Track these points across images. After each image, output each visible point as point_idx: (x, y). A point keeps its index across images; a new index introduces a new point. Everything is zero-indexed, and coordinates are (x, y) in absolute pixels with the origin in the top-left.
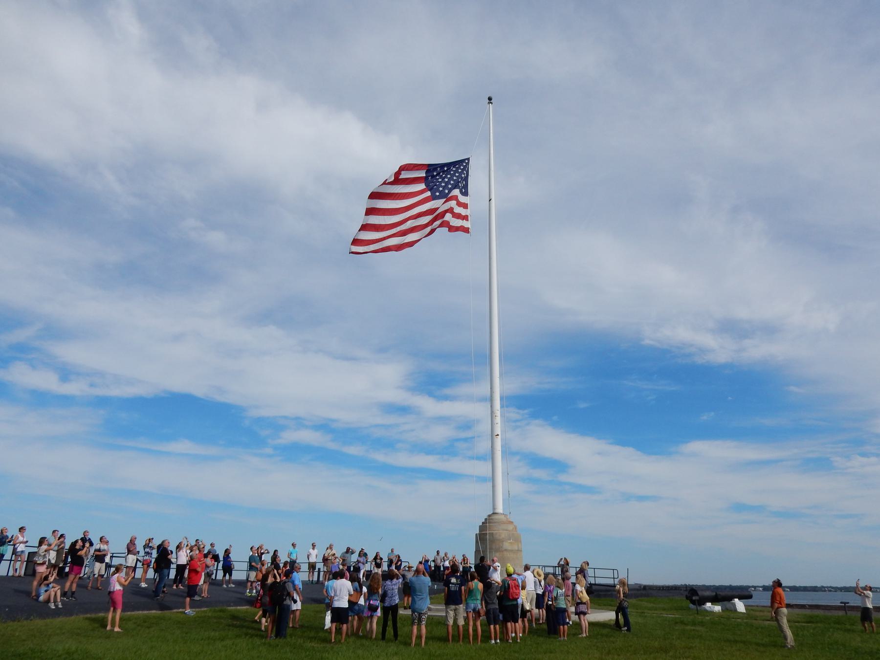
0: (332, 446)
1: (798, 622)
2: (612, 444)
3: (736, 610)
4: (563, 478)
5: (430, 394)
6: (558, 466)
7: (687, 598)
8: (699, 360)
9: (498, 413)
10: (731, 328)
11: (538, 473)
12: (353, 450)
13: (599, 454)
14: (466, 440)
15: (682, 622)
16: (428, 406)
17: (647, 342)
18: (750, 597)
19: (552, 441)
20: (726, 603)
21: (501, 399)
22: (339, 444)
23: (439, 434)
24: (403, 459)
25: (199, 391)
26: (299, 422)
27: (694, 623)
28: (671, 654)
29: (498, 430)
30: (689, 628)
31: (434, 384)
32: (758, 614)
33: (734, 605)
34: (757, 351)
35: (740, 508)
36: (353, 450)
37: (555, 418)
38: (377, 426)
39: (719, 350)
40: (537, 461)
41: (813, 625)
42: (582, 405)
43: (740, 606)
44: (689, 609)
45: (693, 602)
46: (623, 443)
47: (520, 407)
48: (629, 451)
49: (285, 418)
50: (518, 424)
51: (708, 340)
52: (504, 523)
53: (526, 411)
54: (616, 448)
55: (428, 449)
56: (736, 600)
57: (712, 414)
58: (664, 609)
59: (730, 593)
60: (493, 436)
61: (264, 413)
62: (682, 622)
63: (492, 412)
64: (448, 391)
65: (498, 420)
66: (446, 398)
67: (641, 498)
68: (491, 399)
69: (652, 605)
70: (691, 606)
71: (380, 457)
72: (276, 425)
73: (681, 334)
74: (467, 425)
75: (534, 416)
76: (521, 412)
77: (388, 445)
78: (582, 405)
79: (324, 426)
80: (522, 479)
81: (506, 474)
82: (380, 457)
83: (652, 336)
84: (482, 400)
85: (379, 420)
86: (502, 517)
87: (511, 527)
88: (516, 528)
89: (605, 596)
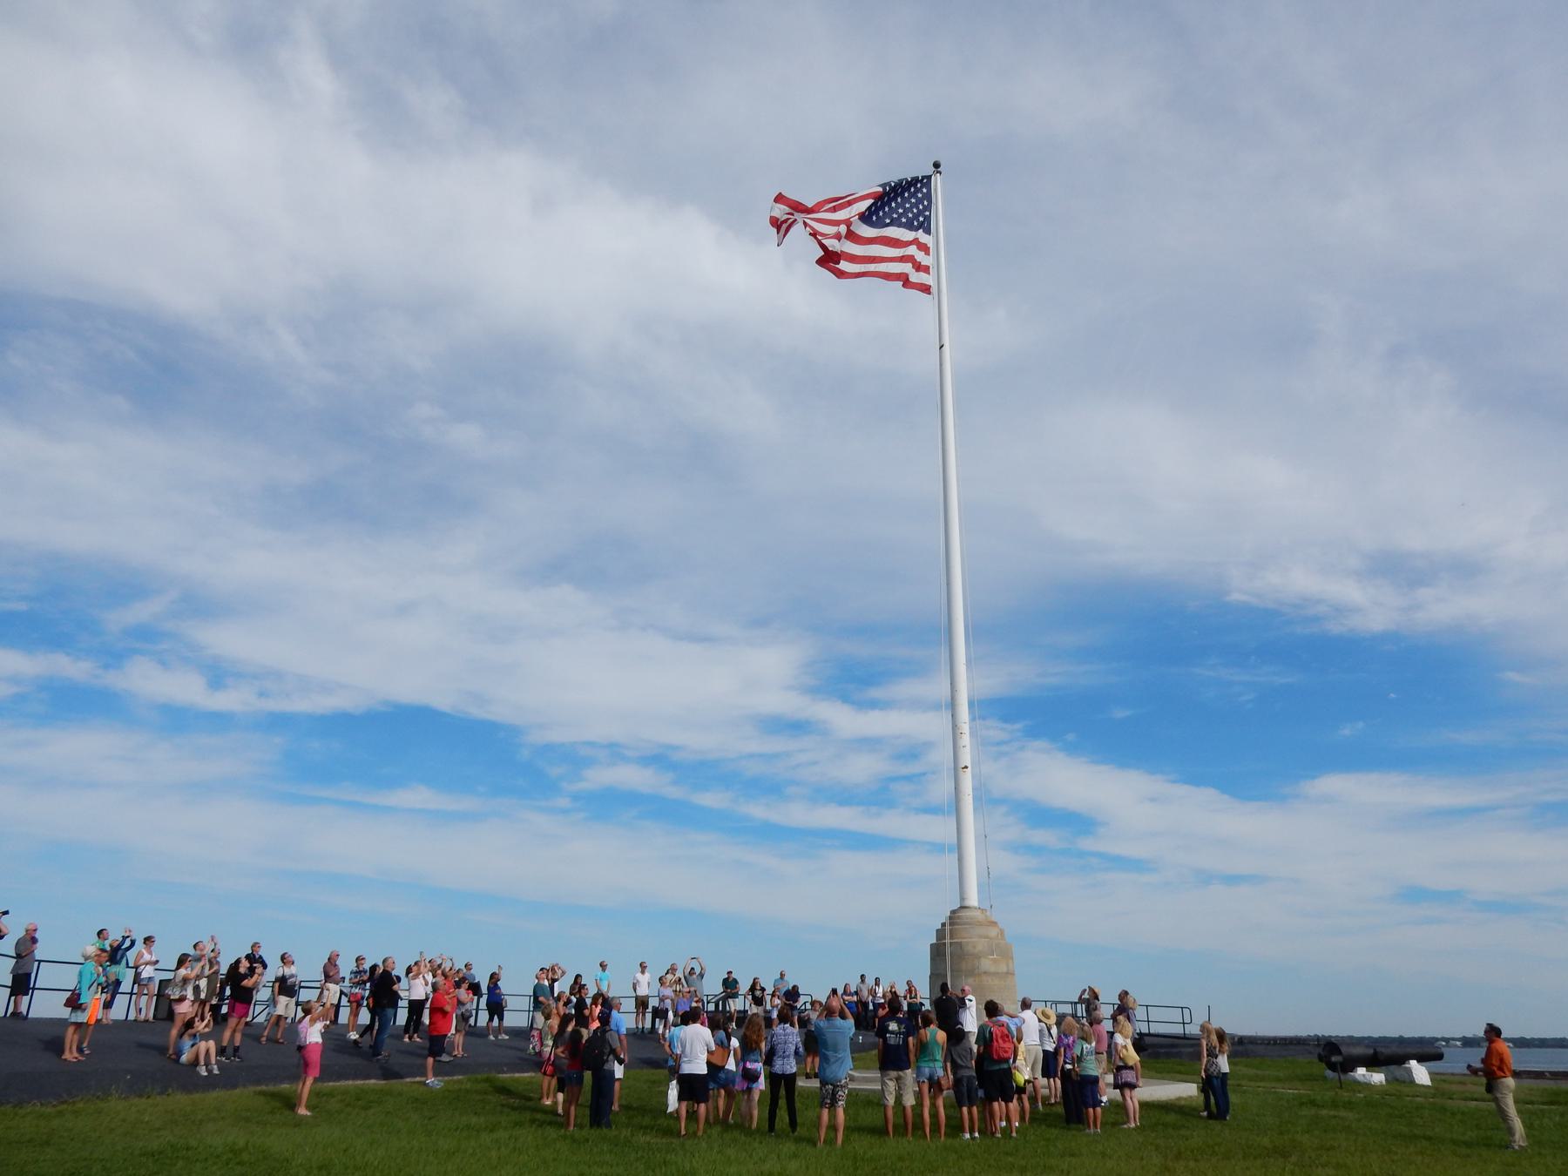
0: (674, 792)
1: (1532, 1103)
2: (1174, 782)
3: (1412, 1081)
4: (1087, 844)
5: (845, 699)
6: (1077, 822)
7: (1321, 1058)
8: (1335, 628)
9: (965, 728)
10: (1390, 567)
11: (1040, 836)
12: (710, 799)
13: (1153, 800)
14: (908, 778)
15: (1313, 1103)
16: (843, 719)
17: (1236, 597)
18: (1439, 1057)
19: (1064, 778)
20: (1392, 1068)
21: (971, 704)
22: (685, 790)
23: (861, 769)
24: (798, 814)
25: (442, 700)
26: (615, 752)
27: (1334, 1105)
28: (1293, 1159)
29: (966, 758)
30: (1324, 1112)
31: (852, 680)
32: (1454, 1088)
33: (1409, 1071)
34: (1442, 608)
35: (1414, 895)
36: (710, 799)
37: (1071, 737)
38: (751, 756)
39: (1372, 608)
40: (1039, 815)
41: (1561, 1108)
42: (1120, 713)
43: (1420, 1073)
44: (1325, 1078)
45: (1332, 1067)
46: (1196, 780)
47: (1006, 719)
48: (1207, 794)
49: (591, 744)
50: (1004, 748)
51: (1351, 592)
52: (980, 924)
53: (1018, 726)
54: (1182, 790)
55: (843, 796)
56: (1413, 1063)
57: (1361, 725)
58: (1278, 1080)
59: (1400, 1051)
60: (957, 769)
61: (554, 736)
62: (1313, 1103)
63: (955, 726)
64: (875, 693)
65: (966, 740)
66: (873, 705)
67: (1232, 880)
68: (953, 705)
69: (1252, 1072)
70: (1329, 1073)
71: (758, 810)
72: (574, 758)
73: (1299, 582)
74: (912, 752)
75: (1032, 733)
76: (1009, 727)
77: (770, 788)
78: (1120, 713)
79: (658, 759)
80: (1017, 848)
81: (983, 839)
82: (758, 810)
83: (1242, 588)
84: (936, 707)
85: (754, 746)
86: (978, 914)
87: (993, 932)
88: (1002, 932)
89: (1168, 1055)
